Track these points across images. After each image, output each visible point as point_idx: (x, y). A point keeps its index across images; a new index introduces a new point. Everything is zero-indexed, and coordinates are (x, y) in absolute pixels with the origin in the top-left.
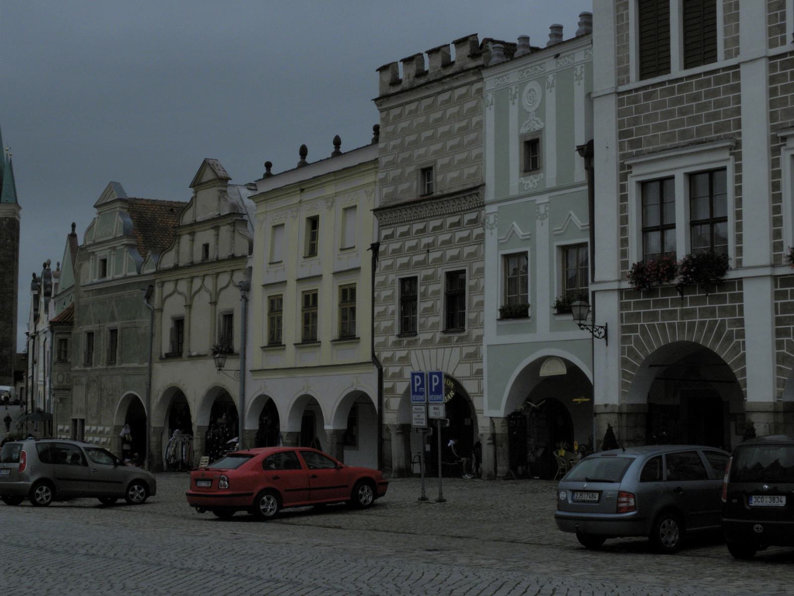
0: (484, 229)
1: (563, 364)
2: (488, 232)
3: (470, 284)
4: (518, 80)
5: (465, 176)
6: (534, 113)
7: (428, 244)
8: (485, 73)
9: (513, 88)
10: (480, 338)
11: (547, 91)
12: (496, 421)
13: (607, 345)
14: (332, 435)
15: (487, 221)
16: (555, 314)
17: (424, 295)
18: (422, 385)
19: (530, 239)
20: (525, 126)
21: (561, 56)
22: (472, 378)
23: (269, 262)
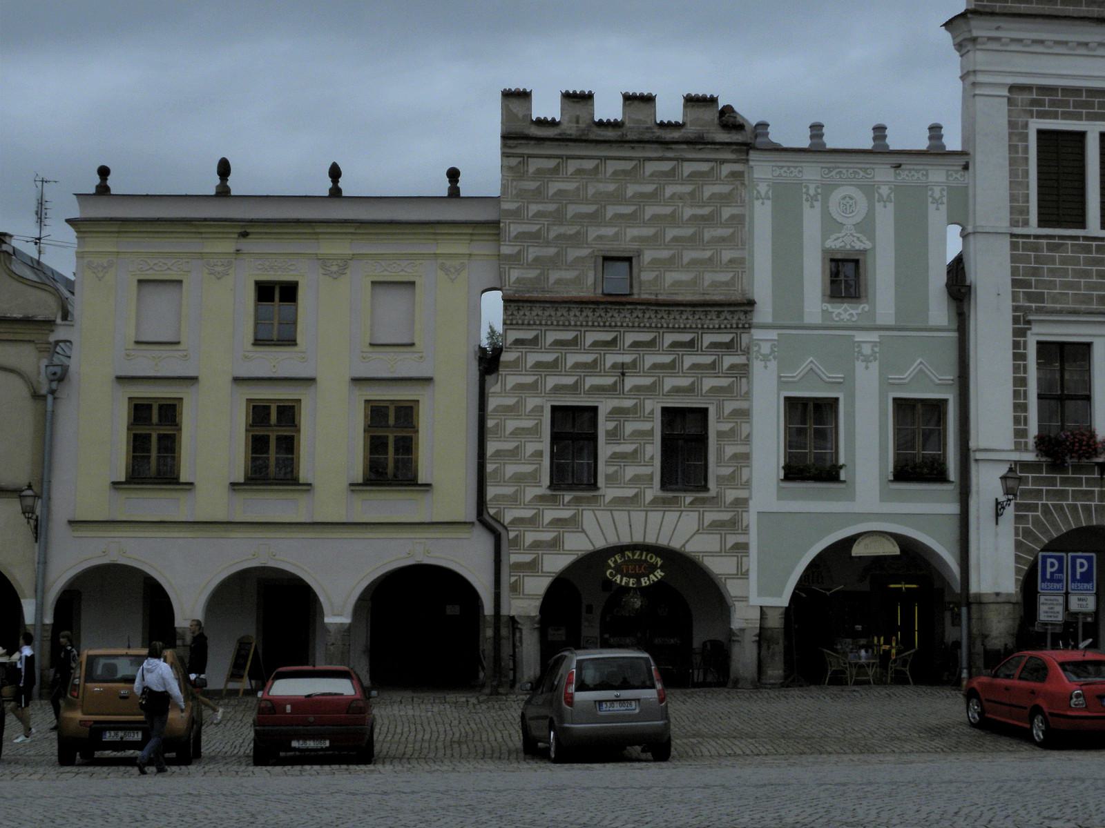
0: (748, 359)
1: (893, 541)
2: (757, 367)
4: (819, 178)
5: (706, 283)
6: (852, 227)
7: (623, 364)
8: (753, 155)
10: (742, 503)
11: (879, 207)
12: (770, 613)
13: (997, 523)
14: (345, 632)
15: (756, 349)
16: (891, 481)
17: (614, 435)
18: (1060, 570)
19: (848, 383)
21: (903, 167)
23: (134, 339)
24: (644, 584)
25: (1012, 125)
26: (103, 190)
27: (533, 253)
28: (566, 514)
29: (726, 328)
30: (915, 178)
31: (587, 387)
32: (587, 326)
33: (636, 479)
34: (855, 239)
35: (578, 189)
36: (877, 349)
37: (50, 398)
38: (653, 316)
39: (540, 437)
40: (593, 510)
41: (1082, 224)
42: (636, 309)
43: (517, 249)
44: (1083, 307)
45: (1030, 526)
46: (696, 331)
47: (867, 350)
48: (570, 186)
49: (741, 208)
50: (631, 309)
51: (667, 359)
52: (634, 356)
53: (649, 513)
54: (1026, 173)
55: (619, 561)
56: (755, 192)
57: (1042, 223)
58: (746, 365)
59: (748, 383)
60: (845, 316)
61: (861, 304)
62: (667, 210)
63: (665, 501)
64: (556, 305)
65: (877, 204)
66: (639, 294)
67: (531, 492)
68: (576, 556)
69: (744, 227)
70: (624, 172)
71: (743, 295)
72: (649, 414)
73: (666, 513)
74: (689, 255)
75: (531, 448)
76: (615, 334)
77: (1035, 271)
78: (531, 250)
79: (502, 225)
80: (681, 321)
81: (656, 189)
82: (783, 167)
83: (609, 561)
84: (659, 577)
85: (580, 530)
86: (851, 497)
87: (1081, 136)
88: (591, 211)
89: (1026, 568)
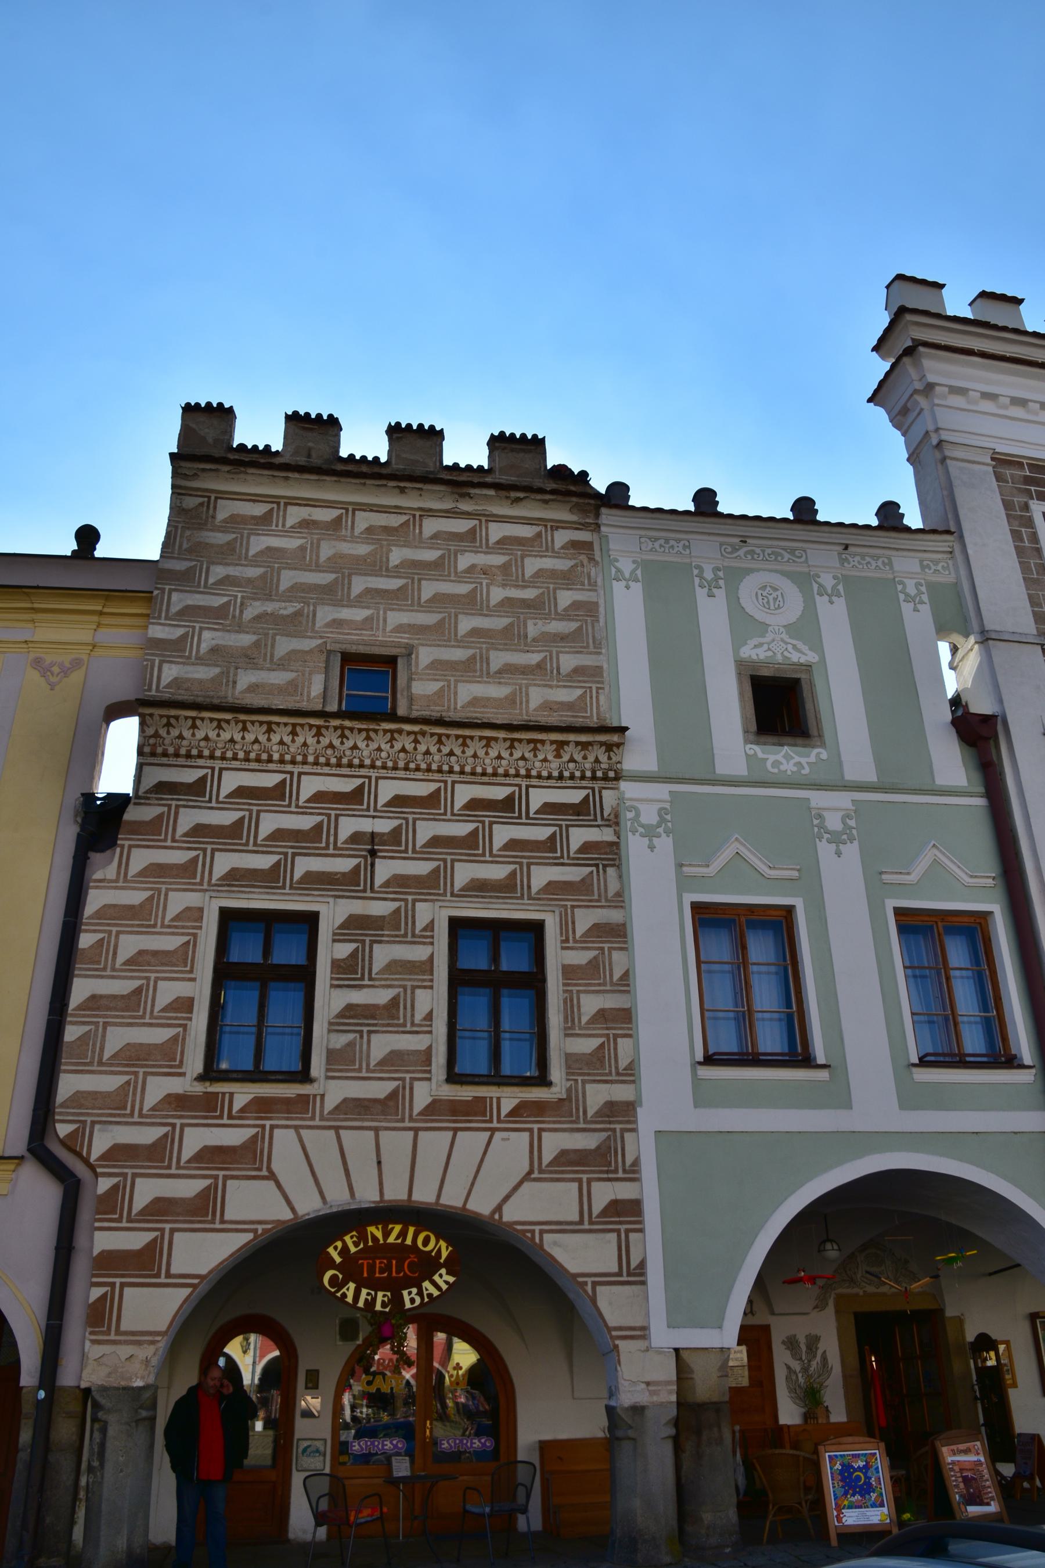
0: (617, 834)
2: (635, 846)
3: (567, 962)
5: (533, 705)
6: (782, 629)
7: (373, 834)
11: (821, 602)
20: (756, 646)
22: (586, 1226)
28: (234, 1137)
29: (572, 777)
31: (298, 875)
32: (305, 763)
33: (394, 1060)
34: (790, 647)
35: (302, 548)
38: (433, 749)
39: (191, 971)
42: (400, 732)
46: (518, 780)
47: (833, 822)
49: (591, 593)
50: (392, 731)
51: (461, 829)
52: (396, 822)
53: (421, 1133)
55: (353, 1249)
56: (613, 570)
58: (616, 844)
59: (620, 877)
60: (789, 767)
61: (814, 747)
64: (242, 717)
65: (817, 597)
68: (250, 1236)
69: (598, 621)
70: (386, 529)
72: (424, 929)
73: (459, 1133)
74: (499, 659)
75: (168, 992)
76: (359, 781)
80: (488, 761)
81: (442, 557)
83: (330, 1250)
84: (444, 1287)
85: (265, 1173)
88: (324, 582)
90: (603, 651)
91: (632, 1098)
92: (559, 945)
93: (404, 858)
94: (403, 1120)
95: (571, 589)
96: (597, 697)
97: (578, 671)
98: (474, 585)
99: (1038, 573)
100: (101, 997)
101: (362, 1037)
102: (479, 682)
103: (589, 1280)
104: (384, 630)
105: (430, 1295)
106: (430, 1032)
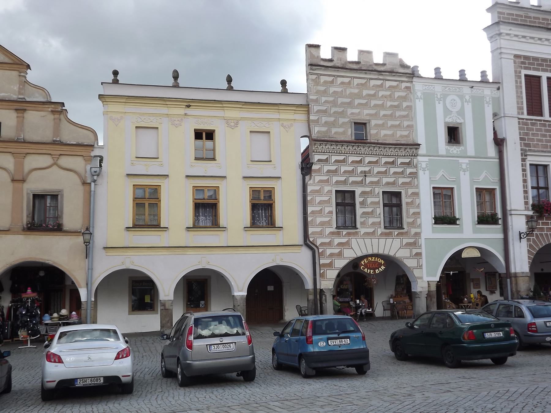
2: (421, 173)
5: (398, 136)
8: (415, 79)
9: (439, 95)
10: (418, 234)
11: (465, 104)
13: (520, 242)
15: (420, 165)
16: (477, 224)
17: (362, 203)
19: (457, 181)
20: (449, 118)
23: (135, 156)
24: (377, 273)
25: (516, 72)
26: (116, 81)
27: (324, 119)
28: (344, 240)
30: (479, 93)
33: (373, 224)
35: (342, 91)
36: (468, 166)
37: (93, 184)
38: (378, 150)
40: (356, 238)
41: (541, 114)
42: (371, 146)
43: (317, 117)
44: (545, 150)
45: (531, 243)
47: (464, 166)
48: (339, 90)
49: (411, 103)
54: (521, 92)
55: (366, 262)
56: (416, 96)
57: (529, 114)
59: (417, 180)
60: (455, 152)
62: (380, 102)
63: (387, 234)
65: (465, 103)
66: (370, 140)
67: (328, 230)
69: (412, 111)
70: (362, 84)
71: (414, 141)
74: (390, 123)
75: (327, 210)
77: (527, 134)
78: (323, 118)
79: (310, 106)
80: (389, 152)
82: (427, 85)
83: (362, 262)
84: (383, 269)
85: (351, 248)
86: (462, 232)
87: (539, 77)
89: (531, 261)
90: (414, 120)
91: (420, 231)
92: (405, 197)
93: (372, 177)
94: (376, 237)
95: (406, 102)
96: (412, 134)
97: (408, 126)
98: (383, 101)
99: (520, 94)
100: (314, 211)
101: (367, 219)
102: (385, 130)
103: (412, 268)
104: (363, 115)
105: (381, 271)
106: (380, 218)
